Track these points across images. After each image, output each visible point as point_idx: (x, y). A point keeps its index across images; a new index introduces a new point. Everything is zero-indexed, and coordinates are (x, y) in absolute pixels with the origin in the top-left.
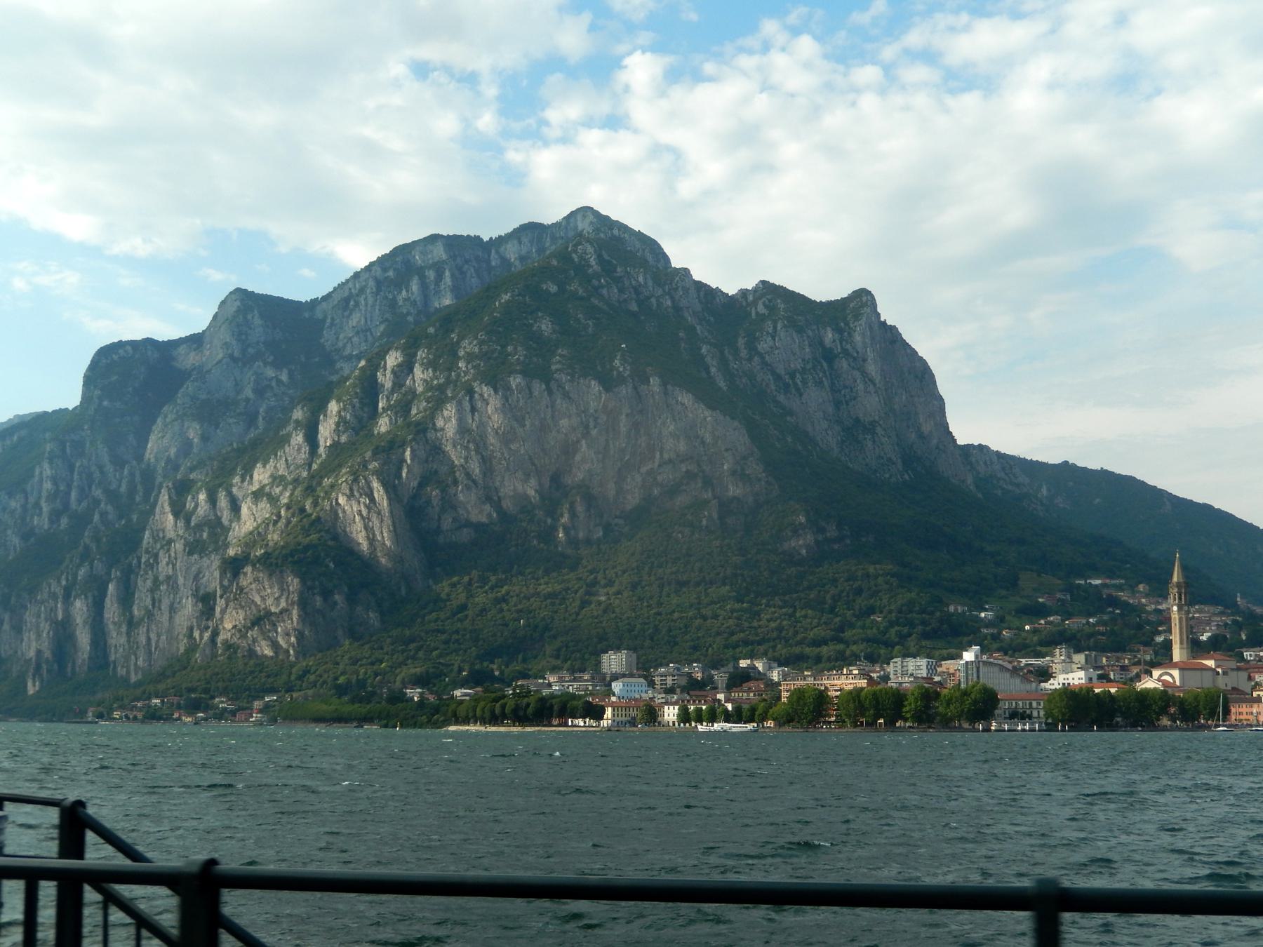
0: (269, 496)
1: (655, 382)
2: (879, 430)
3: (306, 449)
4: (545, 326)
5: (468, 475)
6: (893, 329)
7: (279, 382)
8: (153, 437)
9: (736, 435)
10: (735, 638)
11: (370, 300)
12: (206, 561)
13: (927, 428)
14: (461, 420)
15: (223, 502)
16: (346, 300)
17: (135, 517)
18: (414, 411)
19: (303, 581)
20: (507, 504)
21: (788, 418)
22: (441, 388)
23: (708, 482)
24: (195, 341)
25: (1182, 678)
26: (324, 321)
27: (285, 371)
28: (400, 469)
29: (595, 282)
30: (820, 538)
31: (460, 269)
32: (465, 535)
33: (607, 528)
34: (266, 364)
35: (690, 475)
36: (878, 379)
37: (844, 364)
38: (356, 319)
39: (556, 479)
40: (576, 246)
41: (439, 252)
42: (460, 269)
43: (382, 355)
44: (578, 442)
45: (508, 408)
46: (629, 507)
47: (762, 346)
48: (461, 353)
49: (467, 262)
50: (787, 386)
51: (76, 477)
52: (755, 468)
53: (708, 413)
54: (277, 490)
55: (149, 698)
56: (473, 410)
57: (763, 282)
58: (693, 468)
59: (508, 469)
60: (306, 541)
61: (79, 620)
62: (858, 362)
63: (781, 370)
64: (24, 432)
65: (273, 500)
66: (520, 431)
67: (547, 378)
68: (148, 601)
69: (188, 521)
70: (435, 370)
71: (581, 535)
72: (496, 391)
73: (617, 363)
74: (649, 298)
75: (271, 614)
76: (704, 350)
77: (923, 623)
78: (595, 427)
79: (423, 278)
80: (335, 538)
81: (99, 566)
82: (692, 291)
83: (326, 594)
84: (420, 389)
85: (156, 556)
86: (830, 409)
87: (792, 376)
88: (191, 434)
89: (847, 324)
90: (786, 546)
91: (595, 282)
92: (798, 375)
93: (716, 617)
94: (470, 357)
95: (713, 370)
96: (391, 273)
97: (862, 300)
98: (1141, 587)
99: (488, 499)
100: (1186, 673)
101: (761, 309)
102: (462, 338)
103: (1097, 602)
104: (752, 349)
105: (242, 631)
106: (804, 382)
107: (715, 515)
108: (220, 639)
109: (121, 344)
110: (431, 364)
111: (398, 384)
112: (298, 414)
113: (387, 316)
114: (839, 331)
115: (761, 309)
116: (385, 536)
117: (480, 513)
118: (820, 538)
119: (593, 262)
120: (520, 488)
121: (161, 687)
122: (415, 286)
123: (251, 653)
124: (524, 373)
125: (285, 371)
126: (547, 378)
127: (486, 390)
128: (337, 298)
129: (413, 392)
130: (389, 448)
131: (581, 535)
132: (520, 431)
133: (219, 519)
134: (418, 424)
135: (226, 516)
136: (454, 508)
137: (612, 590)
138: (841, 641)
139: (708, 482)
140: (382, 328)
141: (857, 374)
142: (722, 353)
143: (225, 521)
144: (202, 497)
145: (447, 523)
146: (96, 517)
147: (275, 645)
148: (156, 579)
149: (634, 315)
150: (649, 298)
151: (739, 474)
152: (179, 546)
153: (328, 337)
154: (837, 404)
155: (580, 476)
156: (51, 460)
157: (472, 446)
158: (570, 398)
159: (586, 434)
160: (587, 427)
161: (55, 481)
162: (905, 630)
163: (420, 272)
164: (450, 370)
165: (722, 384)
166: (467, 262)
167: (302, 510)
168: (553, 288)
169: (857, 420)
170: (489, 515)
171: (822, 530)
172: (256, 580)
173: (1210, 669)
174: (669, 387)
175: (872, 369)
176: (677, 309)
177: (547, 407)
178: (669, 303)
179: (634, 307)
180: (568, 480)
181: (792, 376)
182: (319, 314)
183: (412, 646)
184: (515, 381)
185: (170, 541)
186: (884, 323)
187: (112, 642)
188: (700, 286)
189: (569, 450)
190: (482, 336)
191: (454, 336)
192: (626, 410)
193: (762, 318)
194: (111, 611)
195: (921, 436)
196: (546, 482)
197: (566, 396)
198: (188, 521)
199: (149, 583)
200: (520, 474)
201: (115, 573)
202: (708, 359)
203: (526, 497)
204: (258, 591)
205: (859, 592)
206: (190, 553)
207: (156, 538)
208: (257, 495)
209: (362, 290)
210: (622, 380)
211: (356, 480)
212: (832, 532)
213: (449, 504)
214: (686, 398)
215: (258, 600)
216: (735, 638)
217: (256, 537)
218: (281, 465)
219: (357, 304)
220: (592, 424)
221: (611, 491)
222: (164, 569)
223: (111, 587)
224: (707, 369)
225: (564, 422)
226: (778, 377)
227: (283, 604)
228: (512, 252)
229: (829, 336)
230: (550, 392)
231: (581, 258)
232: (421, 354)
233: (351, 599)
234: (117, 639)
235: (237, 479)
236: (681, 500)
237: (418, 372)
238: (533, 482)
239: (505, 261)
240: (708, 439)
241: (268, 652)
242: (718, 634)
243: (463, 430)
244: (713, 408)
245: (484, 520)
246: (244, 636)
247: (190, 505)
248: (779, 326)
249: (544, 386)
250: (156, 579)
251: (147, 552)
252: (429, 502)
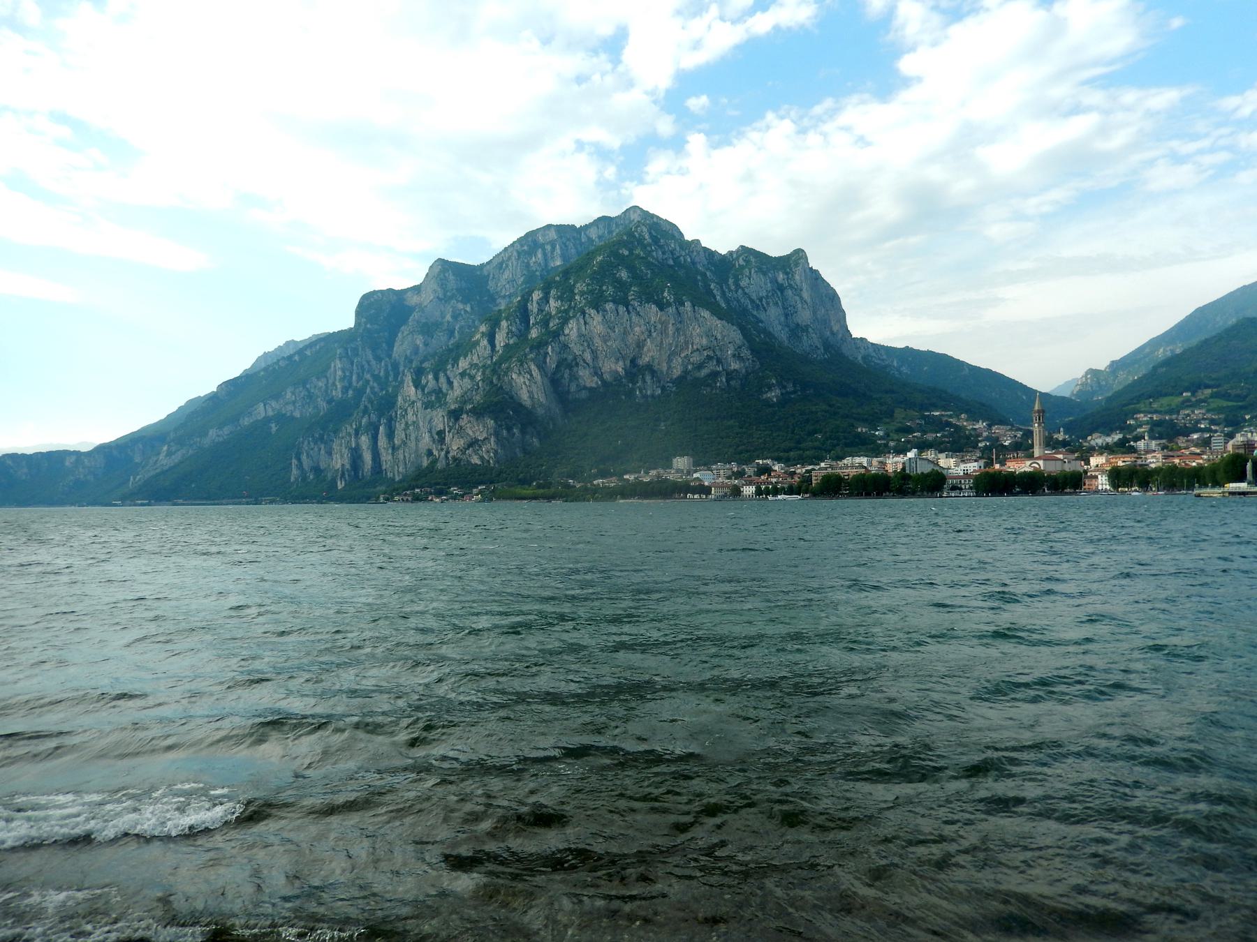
0: (469, 374)
1: (688, 304)
2: (810, 330)
3: (489, 347)
4: (624, 274)
5: (584, 360)
6: (816, 271)
7: (466, 311)
8: (397, 344)
9: (735, 335)
10: (740, 448)
11: (515, 263)
12: (435, 413)
13: (835, 329)
14: (579, 329)
15: (442, 379)
16: (501, 264)
17: (390, 390)
18: (551, 325)
19: (496, 422)
20: (607, 377)
22: (566, 311)
23: (719, 361)
24: (416, 289)
25: (1045, 465)
26: (489, 275)
27: (469, 305)
28: (545, 358)
29: (649, 249)
30: (784, 391)
31: (565, 244)
32: (584, 394)
33: (663, 388)
34: (458, 301)
35: (709, 358)
36: (809, 300)
37: (789, 292)
38: (507, 275)
39: (633, 361)
40: (637, 227)
41: (553, 235)
42: (565, 244)
43: (530, 293)
45: (605, 321)
46: (675, 377)
47: (743, 283)
48: (576, 291)
49: (569, 240)
50: (758, 306)
51: (355, 367)
52: (746, 353)
53: (718, 322)
54: (474, 372)
55: (414, 489)
56: (585, 323)
57: (742, 246)
58: (711, 353)
59: (606, 357)
60: (496, 400)
61: (364, 447)
62: (798, 291)
63: (754, 297)
64: (322, 344)
65: (472, 378)
66: (612, 334)
67: (627, 304)
68: (403, 436)
69: (423, 390)
70: (562, 301)
71: (649, 393)
72: (598, 312)
73: (666, 294)
74: (679, 257)
75: (477, 441)
76: (712, 287)
77: (845, 438)
79: (544, 250)
80: (512, 397)
81: (374, 417)
82: (702, 253)
83: (509, 429)
84: (554, 313)
85: (406, 410)
86: (783, 319)
88: (418, 342)
89: (791, 269)
90: (765, 396)
91: (649, 249)
93: (729, 437)
94: (582, 293)
95: (718, 298)
96: (526, 248)
97: (799, 255)
98: (963, 416)
99: (596, 374)
100: (1048, 462)
101: (741, 262)
102: (576, 282)
103: (940, 425)
104: (738, 286)
105: (463, 451)
106: (768, 303)
107: (724, 380)
108: (450, 455)
109: (374, 292)
110: (557, 298)
111: (541, 310)
112: (483, 328)
113: (525, 272)
114: (787, 274)
115: (741, 262)
116: (541, 397)
117: (592, 382)
118: (784, 391)
119: (647, 236)
120: (613, 367)
121: (420, 483)
122: (540, 255)
123: (469, 462)
124: (614, 301)
125: (469, 305)
126: (627, 304)
127: (593, 312)
128: (495, 263)
129: (549, 314)
130: (540, 345)
131: (649, 393)
132: (612, 334)
133: (440, 389)
134: (554, 332)
135: (444, 387)
136: (577, 379)
137: (669, 423)
138: (800, 449)
139: (719, 361)
140: (522, 279)
141: (797, 298)
142: (722, 287)
143: (444, 391)
144: (430, 377)
145: (573, 388)
146: (368, 390)
147: (482, 458)
148: (407, 423)
149: (671, 266)
150: (679, 257)
151: (737, 356)
152: (419, 404)
153: (491, 285)
154: (786, 315)
155: (647, 359)
156: (340, 359)
157: (585, 344)
159: (650, 335)
161: (343, 370)
162: (835, 442)
163: (542, 246)
164: (571, 301)
165: (724, 305)
166: (569, 240)
167: (492, 382)
168: (626, 253)
169: (798, 325)
170: (597, 383)
171: (785, 387)
172: (470, 422)
173: (1060, 460)
175: (806, 295)
176: (693, 263)
179: (671, 262)
180: (641, 362)
181: (761, 300)
182: (486, 273)
183: (559, 457)
184: (609, 306)
185: (413, 402)
187: (383, 459)
188: (706, 249)
189: (640, 345)
190: (587, 280)
191: (572, 281)
192: (672, 321)
193: (742, 267)
194: (382, 441)
195: (833, 333)
196: (628, 363)
197: (638, 314)
198: (423, 390)
199: (403, 425)
200: (613, 359)
201: (383, 421)
202: (715, 291)
203: (617, 372)
204: (471, 428)
205: (807, 421)
206: (426, 408)
207: (405, 401)
208: (463, 375)
209: (509, 258)
210: (669, 304)
211: (522, 365)
212: (790, 388)
213: (574, 377)
214: (706, 314)
215: (471, 433)
216: (740, 448)
217: (464, 400)
218: (475, 357)
219: (507, 266)
221: (665, 367)
222: (411, 417)
223: (381, 428)
224: (714, 297)
225: (637, 329)
226: (752, 301)
227: (485, 435)
228: (593, 234)
229: (781, 277)
230: (629, 312)
231: (640, 235)
232: (553, 292)
233: (523, 432)
234: (386, 457)
235: (449, 366)
236: (704, 372)
237: (552, 302)
238: (621, 363)
239: (590, 240)
240: (719, 337)
241: (479, 462)
242: (730, 446)
243: (581, 335)
244: (720, 319)
245: (594, 385)
246: (464, 453)
247: (424, 382)
248: (753, 271)
250: (407, 423)
251: (401, 408)
252: (562, 376)
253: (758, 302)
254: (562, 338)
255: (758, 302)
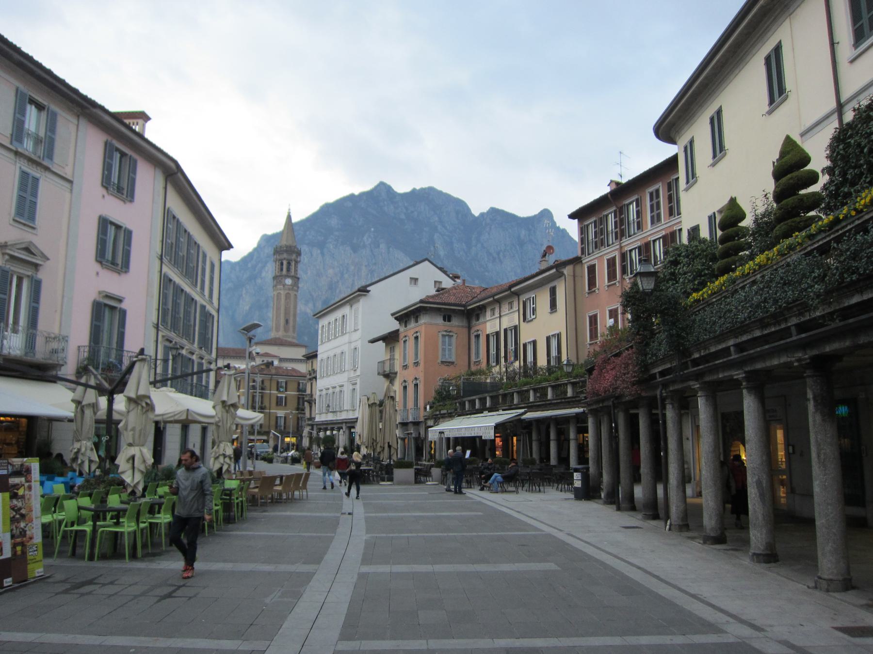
1: (383, 246)
21: (486, 274)
44: (338, 282)
73: (365, 238)
78: (346, 273)
87: (498, 254)
92: (501, 253)
158: (333, 257)
160: (342, 274)
174: (391, 249)
177: (321, 263)
178: (437, 219)
179: (403, 216)
181: (498, 254)
186: (559, 228)
220: (345, 272)
230: (323, 254)
238: (311, 305)
248: (492, 227)
249: (319, 251)
253: (495, 255)
254: (259, 281)
255: (495, 255)
